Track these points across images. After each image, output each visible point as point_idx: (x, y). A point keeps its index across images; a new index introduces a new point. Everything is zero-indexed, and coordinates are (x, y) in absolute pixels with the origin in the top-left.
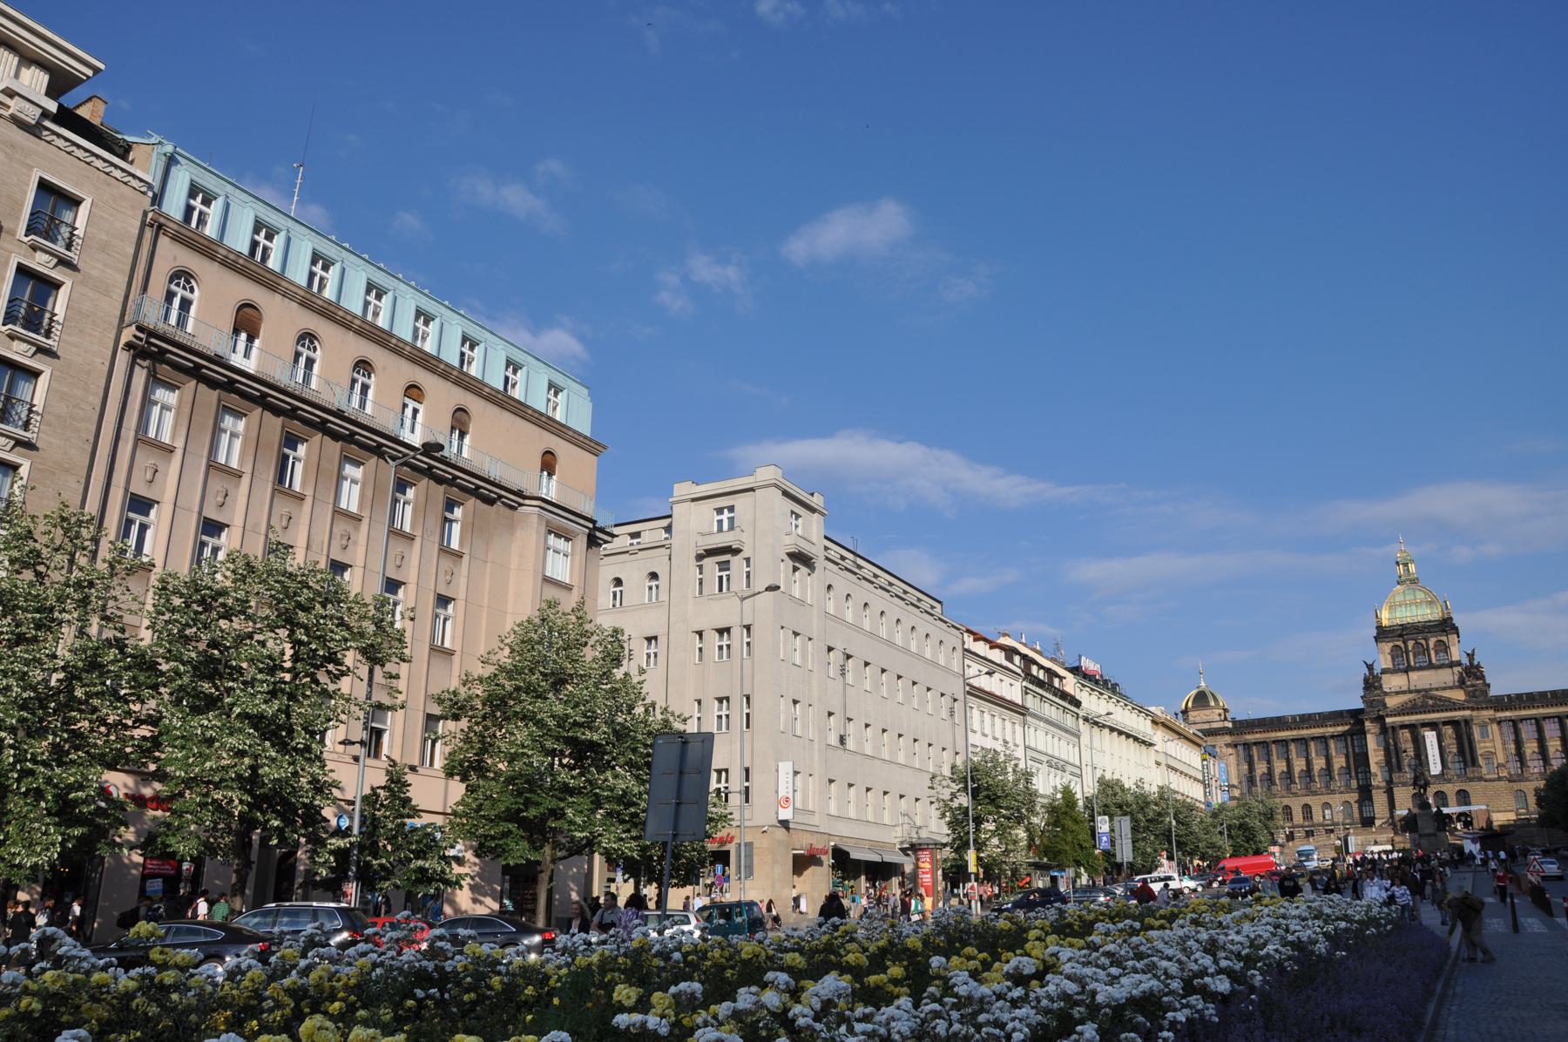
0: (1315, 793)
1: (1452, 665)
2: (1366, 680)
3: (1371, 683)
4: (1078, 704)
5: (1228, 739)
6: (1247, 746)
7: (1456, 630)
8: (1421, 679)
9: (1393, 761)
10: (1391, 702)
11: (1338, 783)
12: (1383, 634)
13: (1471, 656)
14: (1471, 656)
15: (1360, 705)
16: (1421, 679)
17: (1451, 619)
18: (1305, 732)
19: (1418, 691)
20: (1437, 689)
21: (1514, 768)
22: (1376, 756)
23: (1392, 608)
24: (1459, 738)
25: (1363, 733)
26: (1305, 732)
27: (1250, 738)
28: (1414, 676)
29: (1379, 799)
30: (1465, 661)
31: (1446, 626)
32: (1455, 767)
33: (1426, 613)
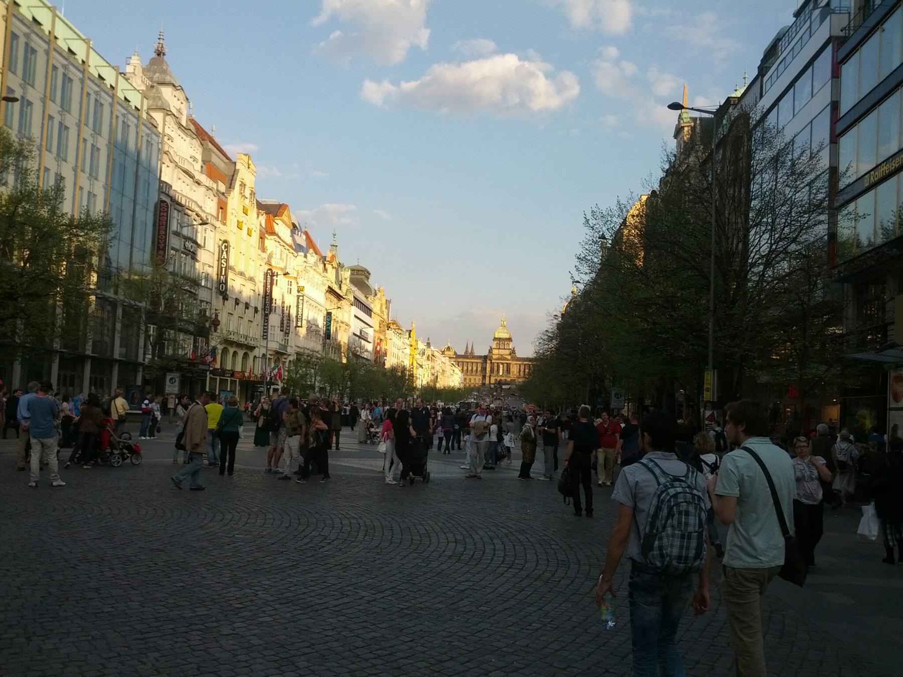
0: (471, 375)
1: (509, 349)
3: (490, 351)
5: (454, 360)
6: (458, 362)
7: (512, 341)
8: (502, 352)
9: (492, 370)
11: (479, 373)
12: (495, 339)
14: (514, 348)
16: (502, 352)
18: (472, 361)
21: (518, 374)
22: (488, 369)
23: (498, 333)
24: (507, 367)
25: (486, 362)
26: (472, 361)
27: (459, 360)
28: (500, 350)
29: (487, 379)
31: (510, 339)
32: (505, 373)
33: (506, 336)
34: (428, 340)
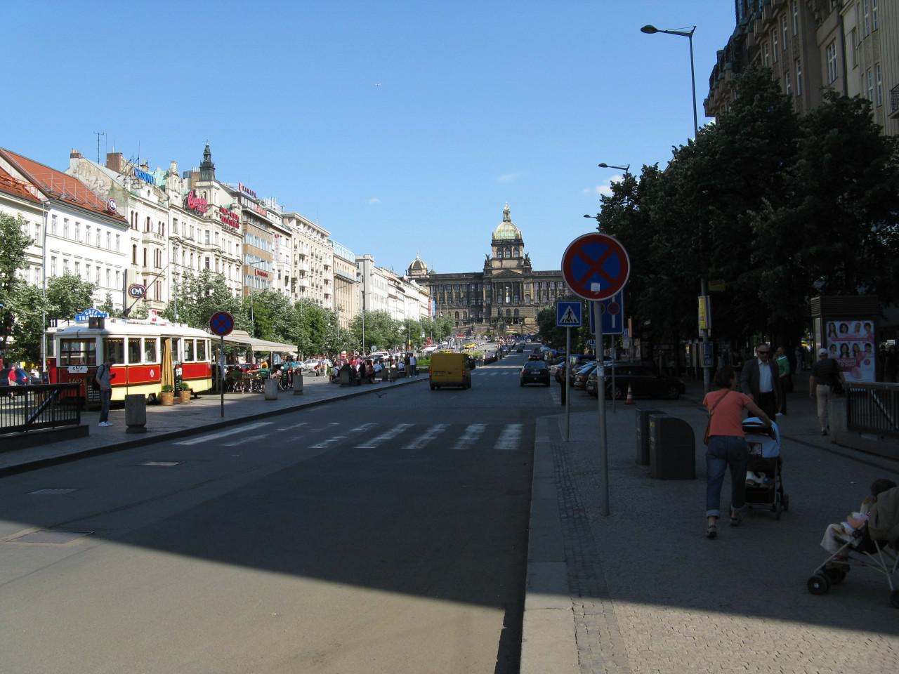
2: (486, 262)
3: (488, 264)
4: (404, 291)
7: (523, 244)
10: (494, 272)
13: (527, 256)
14: (527, 256)
15: (482, 271)
16: (507, 264)
17: (521, 239)
18: (459, 283)
19: (505, 269)
20: (513, 269)
26: (459, 283)
28: (504, 262)
30: (524, 258)
31: (518, 242)
34: (207, 155)
